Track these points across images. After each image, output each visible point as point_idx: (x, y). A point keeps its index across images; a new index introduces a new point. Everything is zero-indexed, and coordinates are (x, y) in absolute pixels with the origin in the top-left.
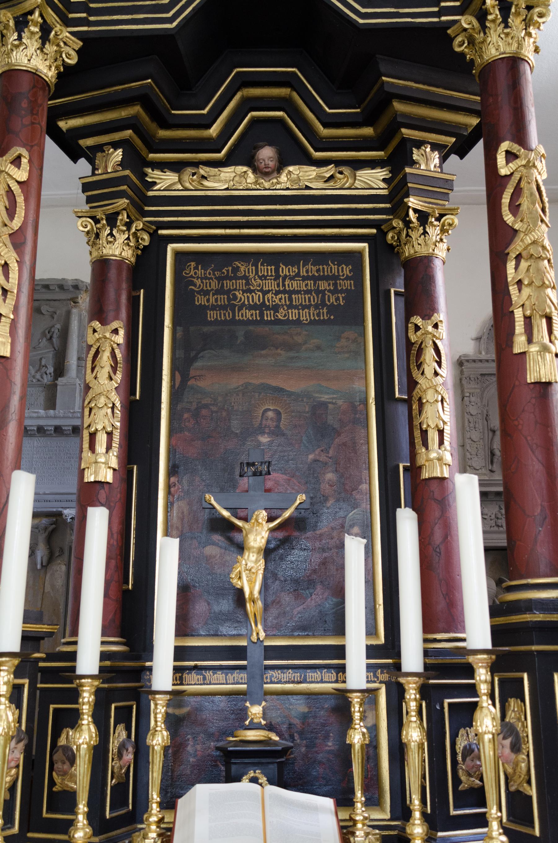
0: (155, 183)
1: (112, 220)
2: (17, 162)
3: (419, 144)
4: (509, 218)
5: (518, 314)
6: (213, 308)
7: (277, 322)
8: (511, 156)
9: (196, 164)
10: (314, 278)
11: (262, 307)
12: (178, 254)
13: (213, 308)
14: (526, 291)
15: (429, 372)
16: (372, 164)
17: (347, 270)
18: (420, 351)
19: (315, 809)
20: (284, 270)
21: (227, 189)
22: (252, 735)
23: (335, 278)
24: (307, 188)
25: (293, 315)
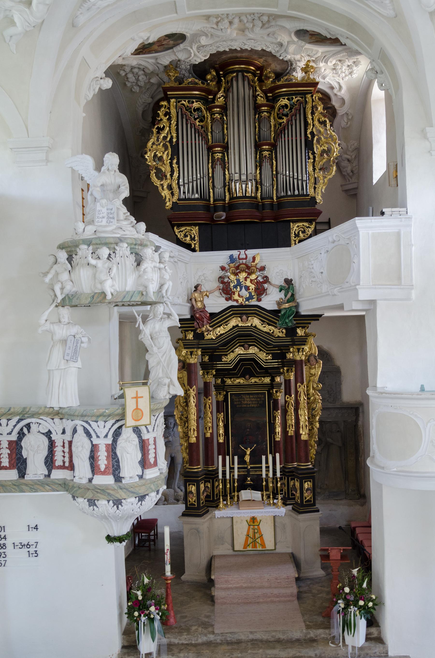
0: (226, 382)
1: (220, 393)
2: (210, 400)
3: (276, 376)
4: (287, 408)
5: (288, 424)
6: (238, 404)
7: (250, 407)
8: (288, 398)
9: (234, 378)
10: (257, 398)
11: (247, 404)
12: (230, 394)
13: (238, 404)
14: (290, 421)
15: (277, 422)
16: (268, 377)
17: (263, 396)
18: (276, 417)
19: (258, 493)
20: (251, 396)
21: (240, 383)
22: (248, 482)
23: (261, 398)
24: (255, 382)
25: (253, 406)
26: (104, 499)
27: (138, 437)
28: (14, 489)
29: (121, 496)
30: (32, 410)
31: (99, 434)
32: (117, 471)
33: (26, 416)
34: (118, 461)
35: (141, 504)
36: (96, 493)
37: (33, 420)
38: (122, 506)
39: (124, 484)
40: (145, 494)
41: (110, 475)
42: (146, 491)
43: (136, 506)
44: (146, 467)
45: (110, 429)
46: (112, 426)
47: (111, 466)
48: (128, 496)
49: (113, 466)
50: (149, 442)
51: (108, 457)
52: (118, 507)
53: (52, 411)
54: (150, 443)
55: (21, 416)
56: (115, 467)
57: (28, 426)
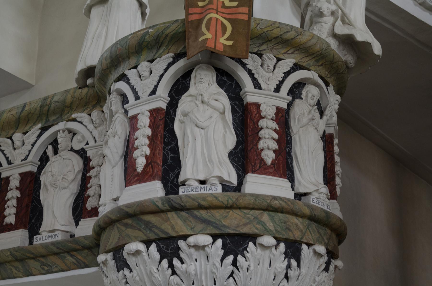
26: (136, 239)
27: (231, 98)
28: (16, 268)
29: (173, 228)
30: (56, 98)
31: (139, 94)
32: (173, 171)
33: (52, 119)
34: (176, 151)
35: (234, 263)
36: (123, 228)
37: (61, 126)
38: (182, 263)
39: (180, 197)
40: (245, 230)
41: (154, 179)
42: (245, 225)
43: (218, 264)
44: (250, 168)
45: (161, 76)
46: (166, 70)
47: (159, 160)
48: (192, 229)
49: (165, 161)
50: (259, 111)
51: (152, 139)
52: (171, 266)
53: (87, 94)
54: (263, 114)
55: (44, 121)
56: (169, 162)
57: (55, 143)
